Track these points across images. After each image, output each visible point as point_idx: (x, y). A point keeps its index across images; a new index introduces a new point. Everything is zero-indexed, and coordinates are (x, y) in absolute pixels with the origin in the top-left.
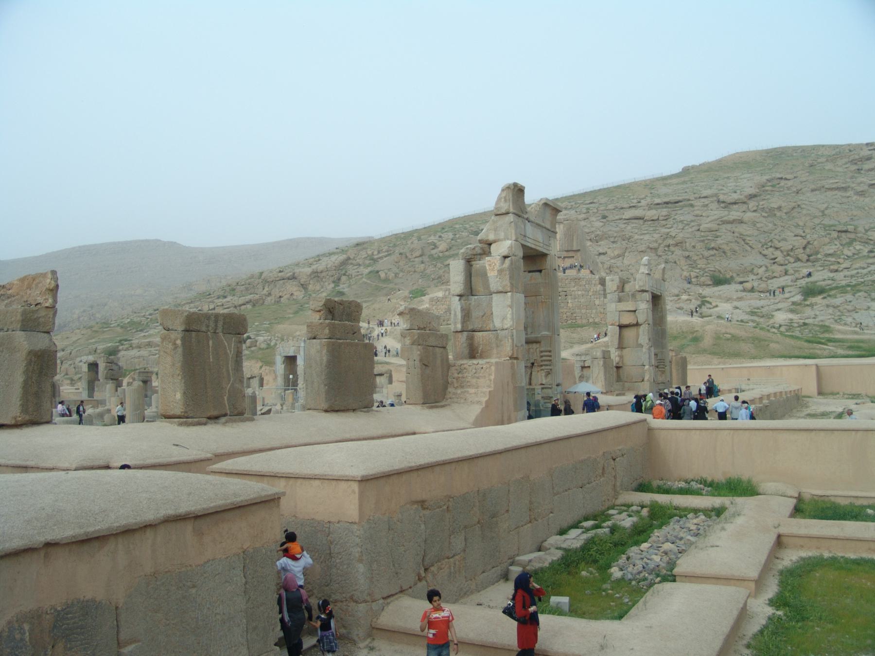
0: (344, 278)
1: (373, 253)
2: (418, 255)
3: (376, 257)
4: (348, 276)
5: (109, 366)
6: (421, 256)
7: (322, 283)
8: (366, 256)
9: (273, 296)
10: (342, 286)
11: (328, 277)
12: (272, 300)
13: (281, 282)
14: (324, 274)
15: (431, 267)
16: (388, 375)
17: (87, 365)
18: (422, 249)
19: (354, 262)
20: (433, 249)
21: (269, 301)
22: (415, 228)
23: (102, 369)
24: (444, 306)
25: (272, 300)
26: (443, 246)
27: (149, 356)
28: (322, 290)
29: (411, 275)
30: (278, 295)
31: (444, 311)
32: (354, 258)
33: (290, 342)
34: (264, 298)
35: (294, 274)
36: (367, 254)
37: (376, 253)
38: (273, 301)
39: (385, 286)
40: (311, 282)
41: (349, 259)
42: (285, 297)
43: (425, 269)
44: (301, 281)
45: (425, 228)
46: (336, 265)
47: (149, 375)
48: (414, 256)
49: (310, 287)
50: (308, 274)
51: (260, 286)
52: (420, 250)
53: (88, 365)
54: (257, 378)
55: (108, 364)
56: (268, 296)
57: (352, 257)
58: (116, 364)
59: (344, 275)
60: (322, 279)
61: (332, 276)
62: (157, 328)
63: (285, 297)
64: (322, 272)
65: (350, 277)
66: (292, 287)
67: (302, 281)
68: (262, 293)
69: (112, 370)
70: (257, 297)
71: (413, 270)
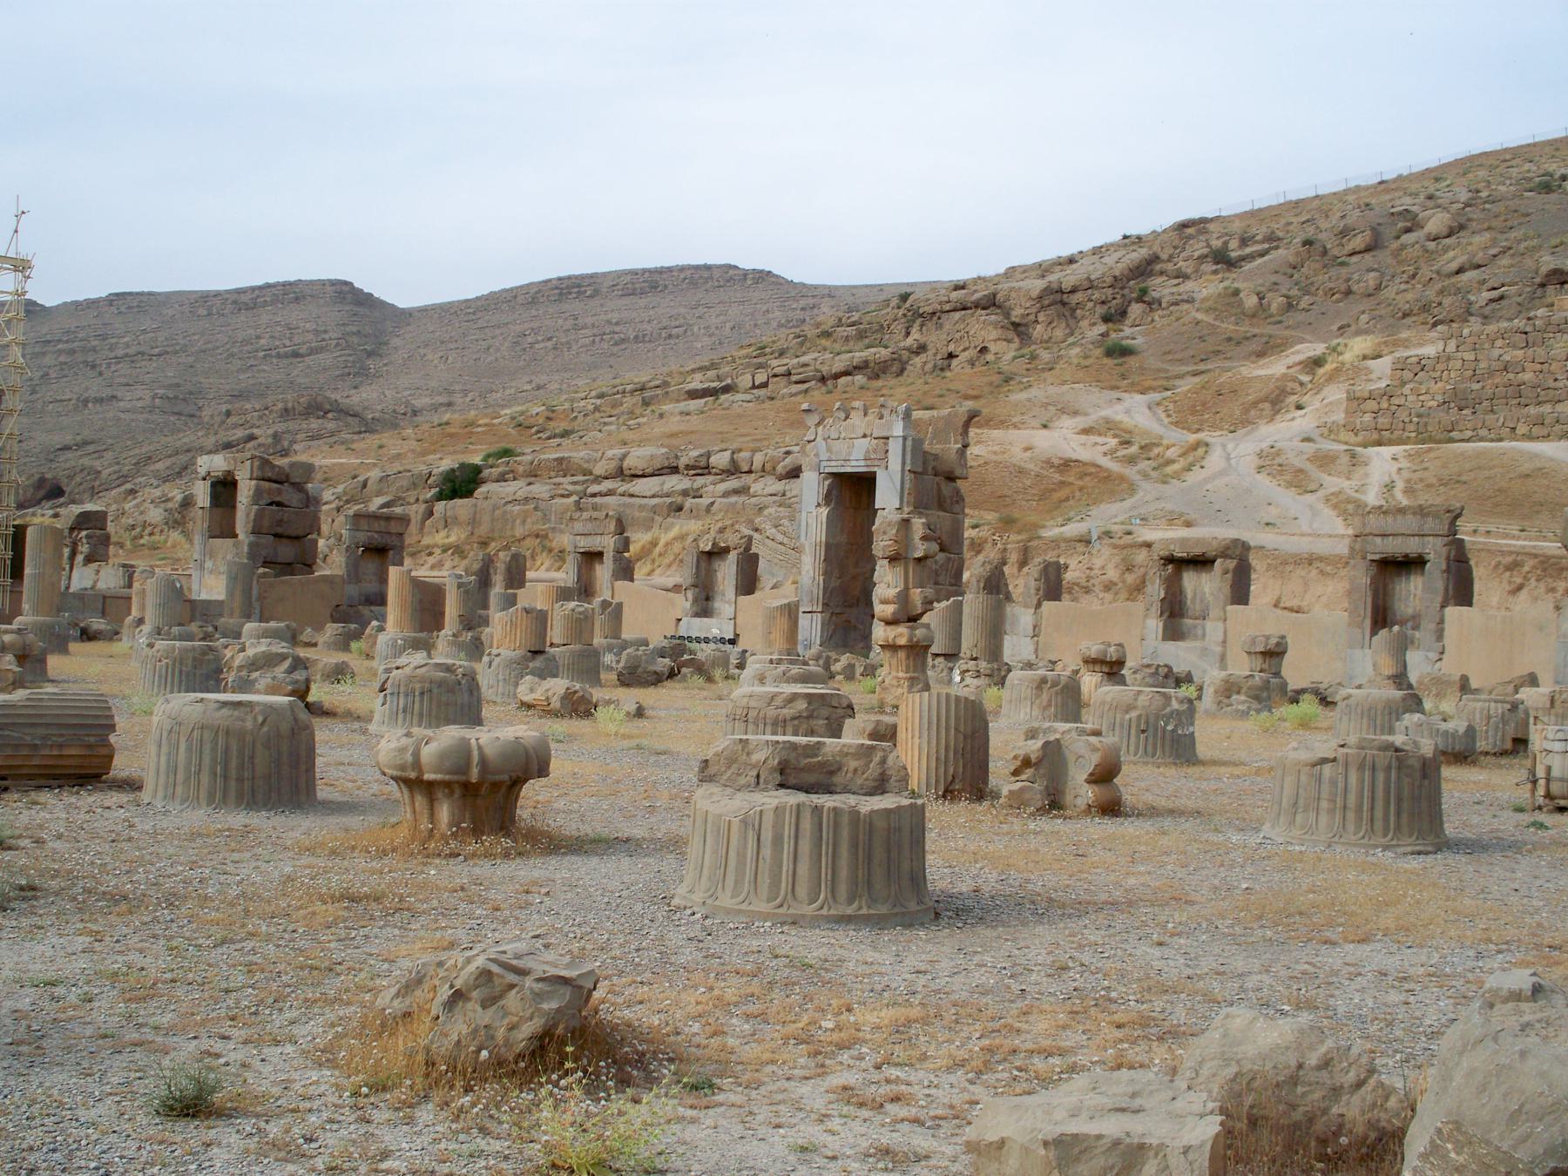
0: (1136, 309)
1: (1226, 243)
2: (1362, 247)
3: (1233, 254)
4: (1149, 304)
5: (270, 492)
6: (1368, 250)
7: (1071, 322)
8: (1206, 251)
9: (930, 353)
10: (1128, 331)
11: (1090, 305)
12: (925, 363)
13: (957, 315)
14: (1078, 297)
15: (1398, 280)
16: (1231, 564)
17: (208, 483)
18: (1373, 229)
19: (1170, 266)
20: (1408, 230)
21: (919, 365)
22: (1352, 184)
23: (244, 501)
24: (1440, 384)
25: (925, 363)
26: (1436, 222)
27: (552, 497)
28: (1071, 340)
29: (1338, 301)
30: (944, 352)
31: (1440, 398)
32: (1171, 257)
33: (856, 418)
34: (905, 358)
35: (994, 295)
36: (1208, 246)
37: (1233, 244)
38: (929, 367)
39: (1256, 331)
40: (1041, 317)
41: (1155, 259)
42: (964, 356)
43: (1378, 288)
44: (1014, 313)
45: (1382, 183)
46: (1117, 273)
47: (394, 527)
48: (1349, 248)
49: (1038, 331)
50: (1035, 294)
51: (898, 328)
52: (1368, 232)
53: (213, 485)
54: (733, 556)
55: (267, 485)
56: (917, 353)
57: (1164, 256)
58: (299, 487)
59: (1140, 300)
60: (1073, 310)
61: (1103, 303)
62: (606, 428)
63: (964, 356)
64: (1073, 291)
65: (1153, 304)
66: (983, 328)
67: (1016, 315)
68: (902, 344)
69: (278, 504)
70: (884, 353)
71: (1343, 287)
